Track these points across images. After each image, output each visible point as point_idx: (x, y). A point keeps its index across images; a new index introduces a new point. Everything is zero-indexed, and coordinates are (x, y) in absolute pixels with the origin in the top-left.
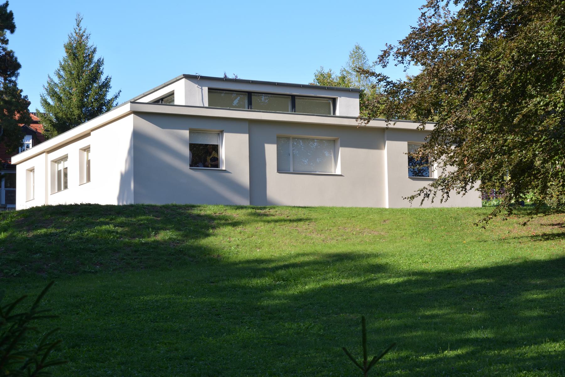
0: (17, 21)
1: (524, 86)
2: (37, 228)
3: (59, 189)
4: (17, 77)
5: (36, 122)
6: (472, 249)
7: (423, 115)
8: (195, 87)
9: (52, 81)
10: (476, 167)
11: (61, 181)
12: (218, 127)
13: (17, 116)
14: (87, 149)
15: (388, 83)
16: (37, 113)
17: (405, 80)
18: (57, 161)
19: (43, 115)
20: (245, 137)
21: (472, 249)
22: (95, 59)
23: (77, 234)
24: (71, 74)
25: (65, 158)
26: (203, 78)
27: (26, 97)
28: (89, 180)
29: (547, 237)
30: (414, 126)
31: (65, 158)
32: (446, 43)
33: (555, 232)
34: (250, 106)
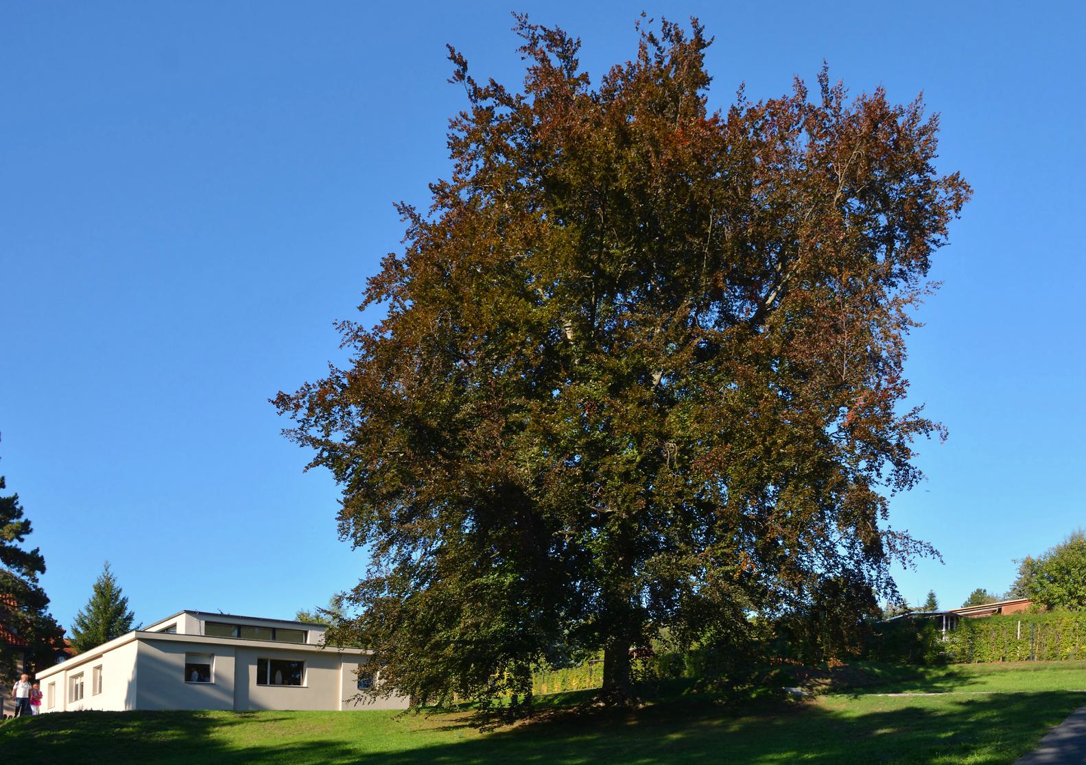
0: (47, 564)
1: (436, 623)
3: (76, 699)
4: (46, 609)
5: (68, 647)
6: (391, 738)
7: (365, 642)
8: (194, 620)
9: (82, 614)
10: (401, 681)
13: (52, 641)
14: (100, 667)
15: (341, 619)
16: (69, 639)
17: (355, 618)
18: (75, 677)
19: (72, 641)
20: (232, 660)
21: (391, 738)
22: (121, 597)
24: (99, 608)
25: (81, 675)
26: (201, 613)
27: (60, 626)
28: (100, 691)
30: (358, 651)
31: (81, 675)
32: (386, 592)
33: (451, 725)
34: (239, 636)
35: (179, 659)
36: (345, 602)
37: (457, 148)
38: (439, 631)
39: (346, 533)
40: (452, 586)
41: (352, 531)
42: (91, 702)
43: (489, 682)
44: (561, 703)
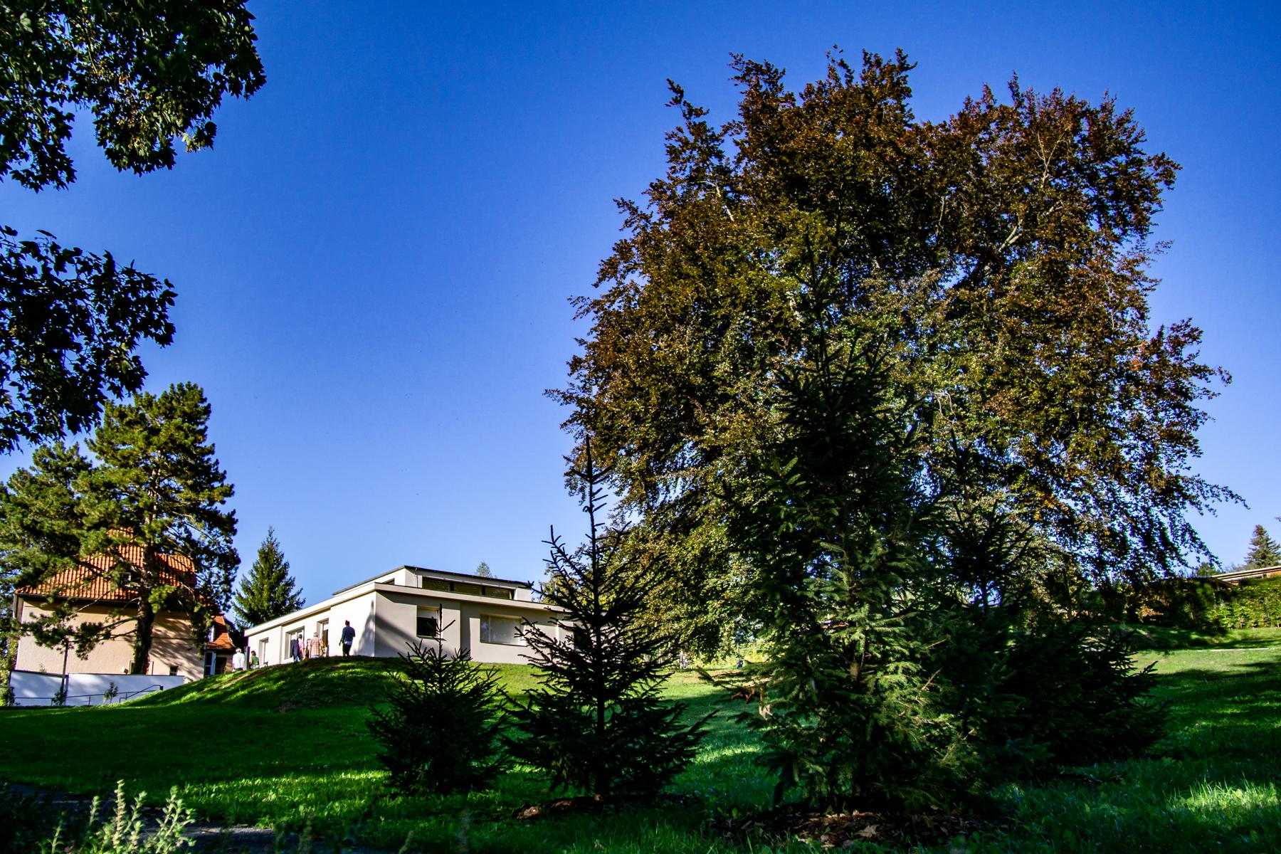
37: (673, 153)
39: (574, 488)
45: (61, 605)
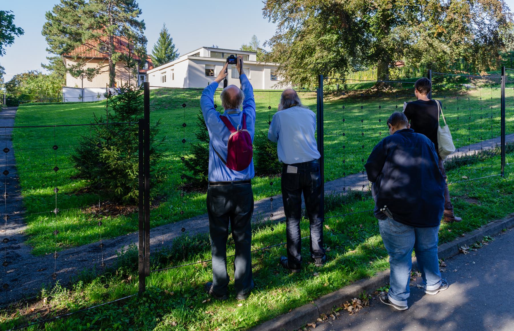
2: (163, 95)
11: (164, 79)
12: (213, 64)
18: (162, 73)
23: (175, 97)
25: (165, 72)
29: (310, 99)
31: (165, 72)
35: (202, 68)
36: (267, 45)
38: (307, 58)
39: (266, 15)
40: (311, 39)
41: (268, 14)
42: (170, 84)
43: (329, 80)
44: (358, 89)
45: (81, 59)
